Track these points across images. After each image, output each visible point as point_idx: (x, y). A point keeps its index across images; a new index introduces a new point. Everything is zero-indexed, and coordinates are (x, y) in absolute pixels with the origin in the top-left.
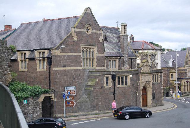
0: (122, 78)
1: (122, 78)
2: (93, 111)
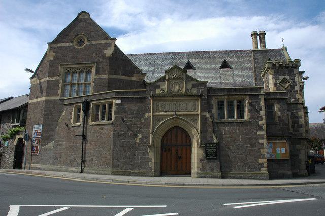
0: (104, 107)
1: (104, 107)
2: (54, 164)
